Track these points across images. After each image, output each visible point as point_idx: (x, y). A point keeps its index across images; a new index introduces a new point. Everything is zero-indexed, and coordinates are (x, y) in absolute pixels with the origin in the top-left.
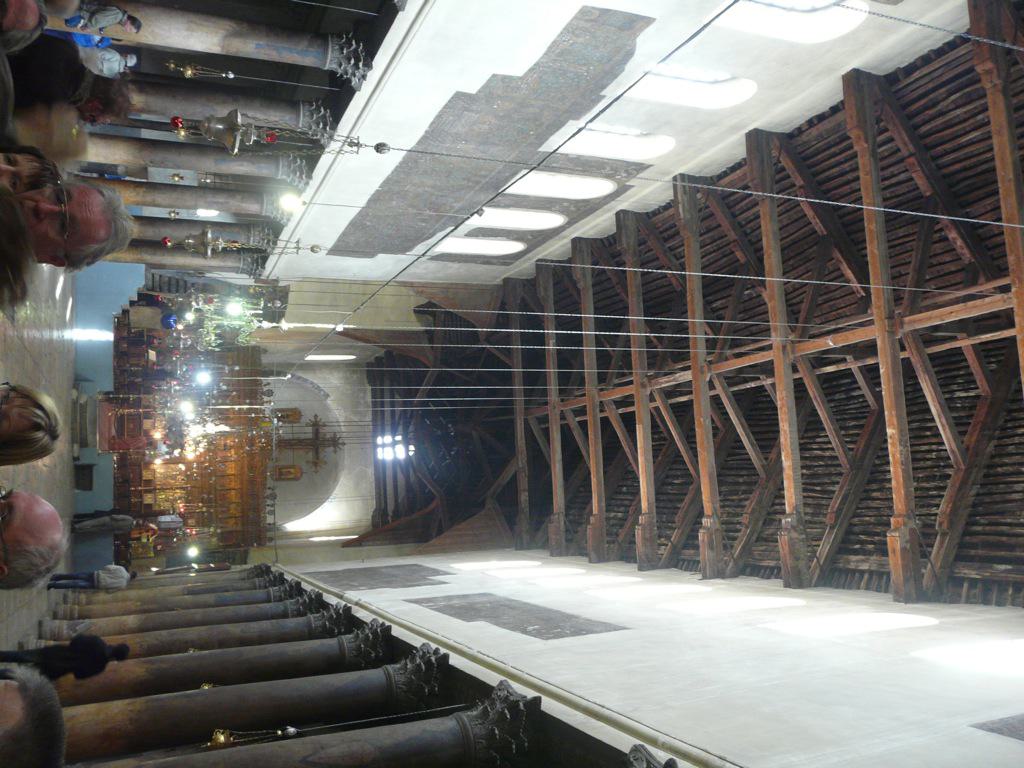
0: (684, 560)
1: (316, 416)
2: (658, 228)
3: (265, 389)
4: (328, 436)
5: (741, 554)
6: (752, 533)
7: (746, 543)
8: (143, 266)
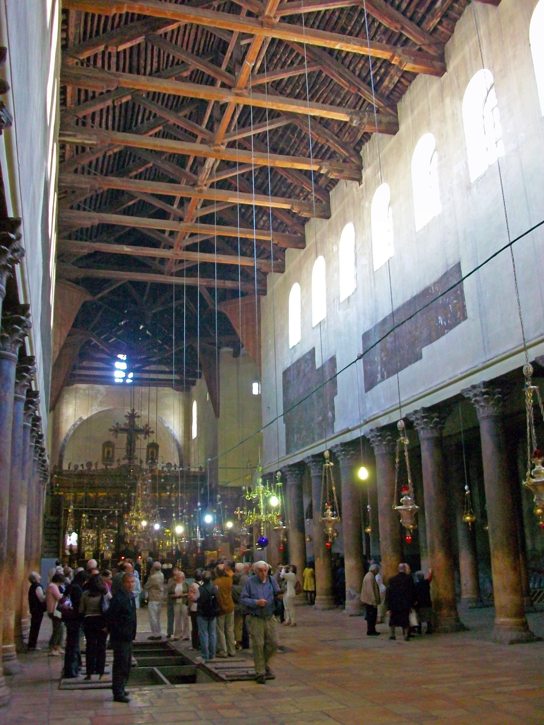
0: (327, 186)
1: (110, 430)
2: (73, 155)
3: (85, 468)
4: (127, 422)
5: (347, 151)
6: (332, 139)
7: (339, 145)
8: (43, 559)
